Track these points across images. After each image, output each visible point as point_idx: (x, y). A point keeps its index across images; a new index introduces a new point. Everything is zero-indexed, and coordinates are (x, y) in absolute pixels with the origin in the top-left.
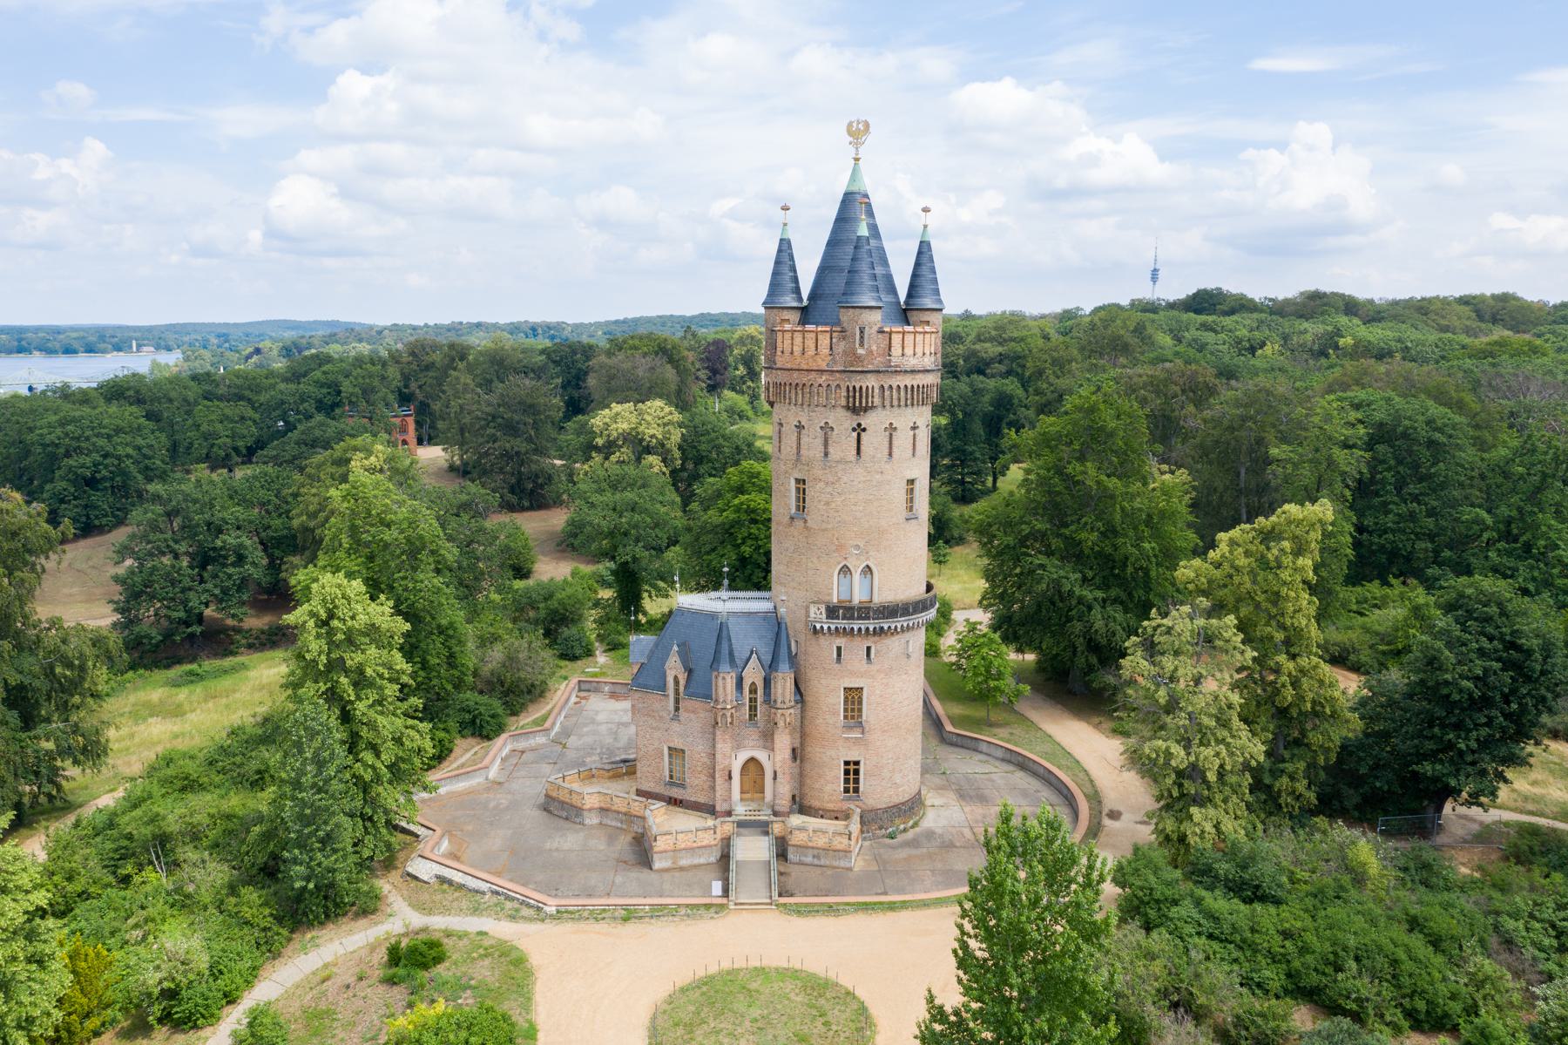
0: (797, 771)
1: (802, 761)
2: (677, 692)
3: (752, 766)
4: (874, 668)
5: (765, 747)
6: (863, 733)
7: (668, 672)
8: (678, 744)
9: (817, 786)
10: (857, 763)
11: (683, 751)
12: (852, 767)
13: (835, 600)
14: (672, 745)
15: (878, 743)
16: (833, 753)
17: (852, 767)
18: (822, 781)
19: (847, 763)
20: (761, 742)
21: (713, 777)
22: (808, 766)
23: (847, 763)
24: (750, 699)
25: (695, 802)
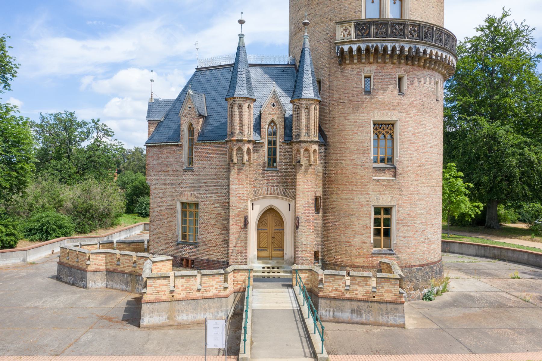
0: (320, 223)
1: (325, 212)
2: (191, 140)
3: (270, 219)
4: (407, 100)
5: (285, 195)
6: (395, 175)
7: (183, 119)
8: (190, 197)
9: (344, 239)
10: (388, 210)
11: (196, 205)
12: (382, 216)
13: (363, 17)
14: (184, 200)
15: (412, 189)
16: (362, 198)
17: (382, 216)
18: (349, 232)
19: (377, 211)
20: (280, 189)
21: (226, 228)
22: (332, 217)
23: (377, 211)
24: (269, 142)
25: (207, 260)
